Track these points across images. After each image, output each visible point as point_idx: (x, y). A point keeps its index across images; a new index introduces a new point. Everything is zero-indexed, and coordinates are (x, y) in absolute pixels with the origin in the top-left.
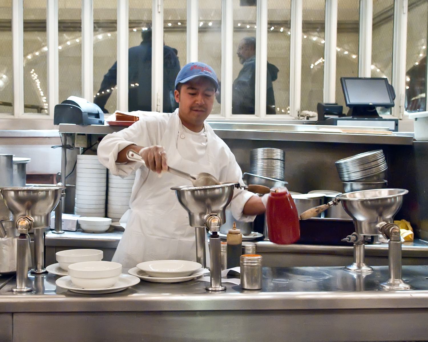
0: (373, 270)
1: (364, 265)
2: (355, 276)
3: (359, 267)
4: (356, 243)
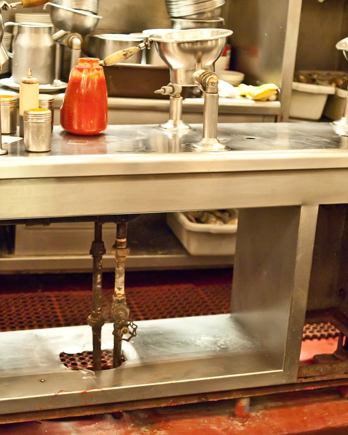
0: (190, 128)
1: (181, 122)
2: (170, 136)
3: (175, 125)
4: (172, 95)
